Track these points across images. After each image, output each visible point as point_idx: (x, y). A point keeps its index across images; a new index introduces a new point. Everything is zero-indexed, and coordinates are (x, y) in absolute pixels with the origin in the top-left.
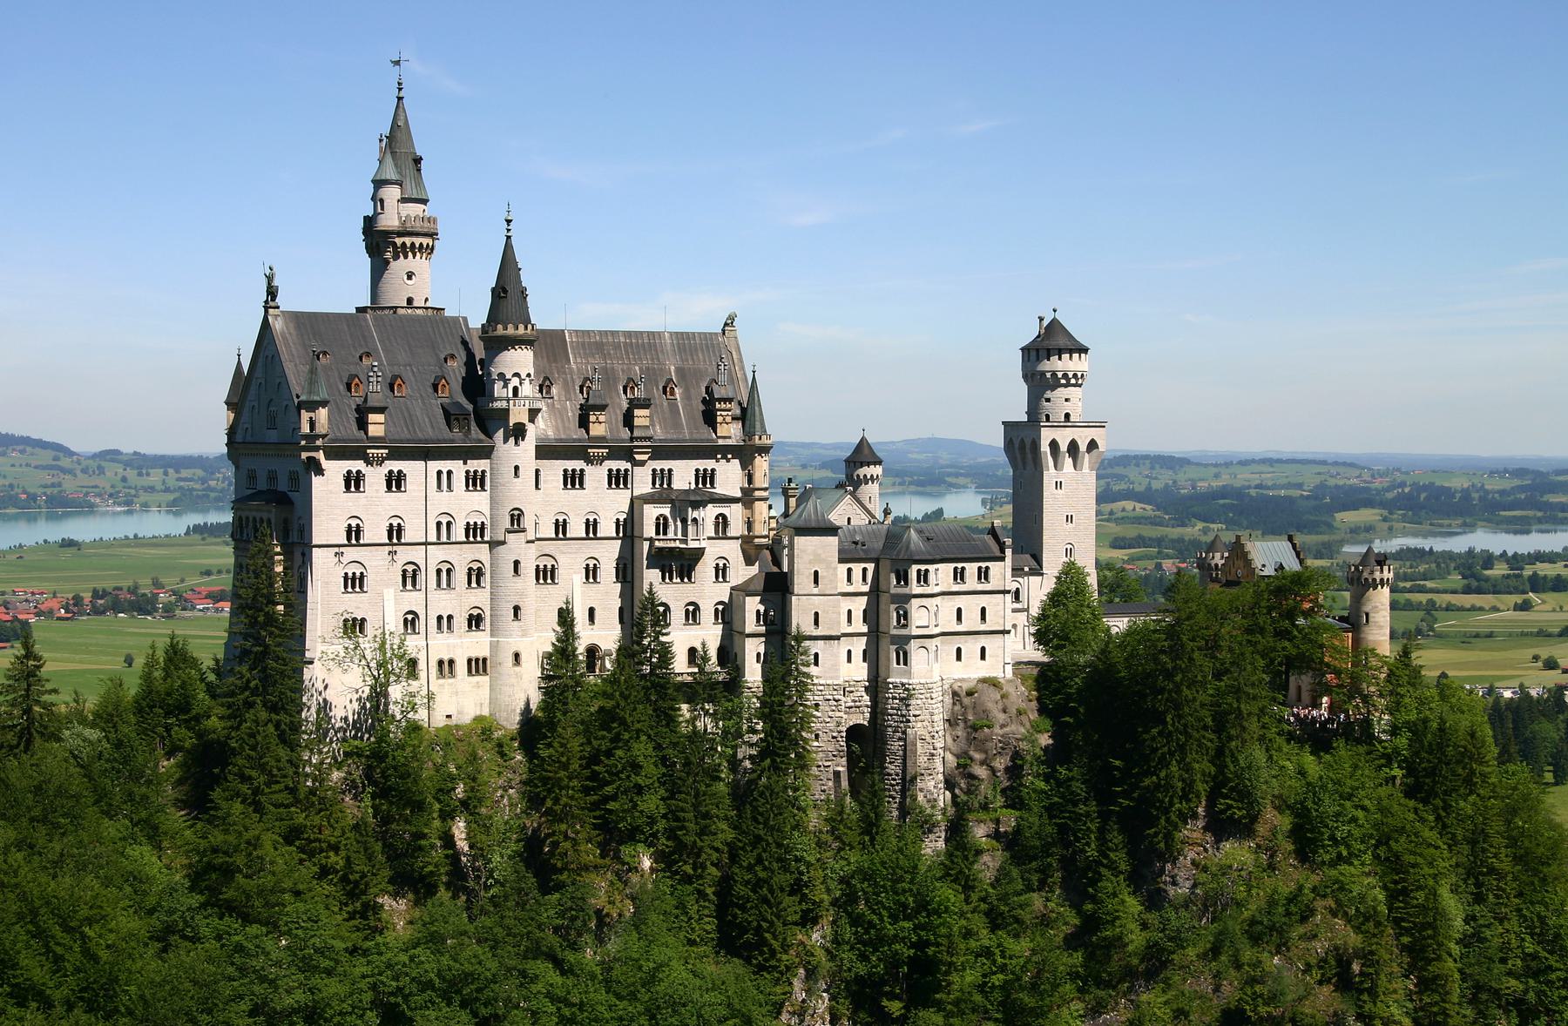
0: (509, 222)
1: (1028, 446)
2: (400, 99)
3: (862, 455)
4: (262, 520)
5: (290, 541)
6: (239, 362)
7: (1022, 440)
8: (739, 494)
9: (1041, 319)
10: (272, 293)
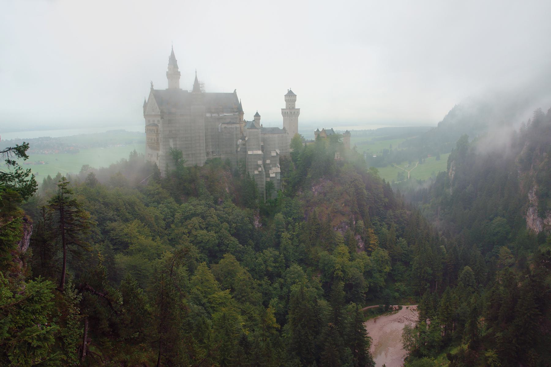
0: (196, 72)
1: (286, 113)
2: (172, 49)
3: (257, 115)
4: (152, 129)
5: (158, 133)
6: (145, 101)
7: (285, 113)
8: (238, 122)
9: (288, 90)
10: (152, 86)
